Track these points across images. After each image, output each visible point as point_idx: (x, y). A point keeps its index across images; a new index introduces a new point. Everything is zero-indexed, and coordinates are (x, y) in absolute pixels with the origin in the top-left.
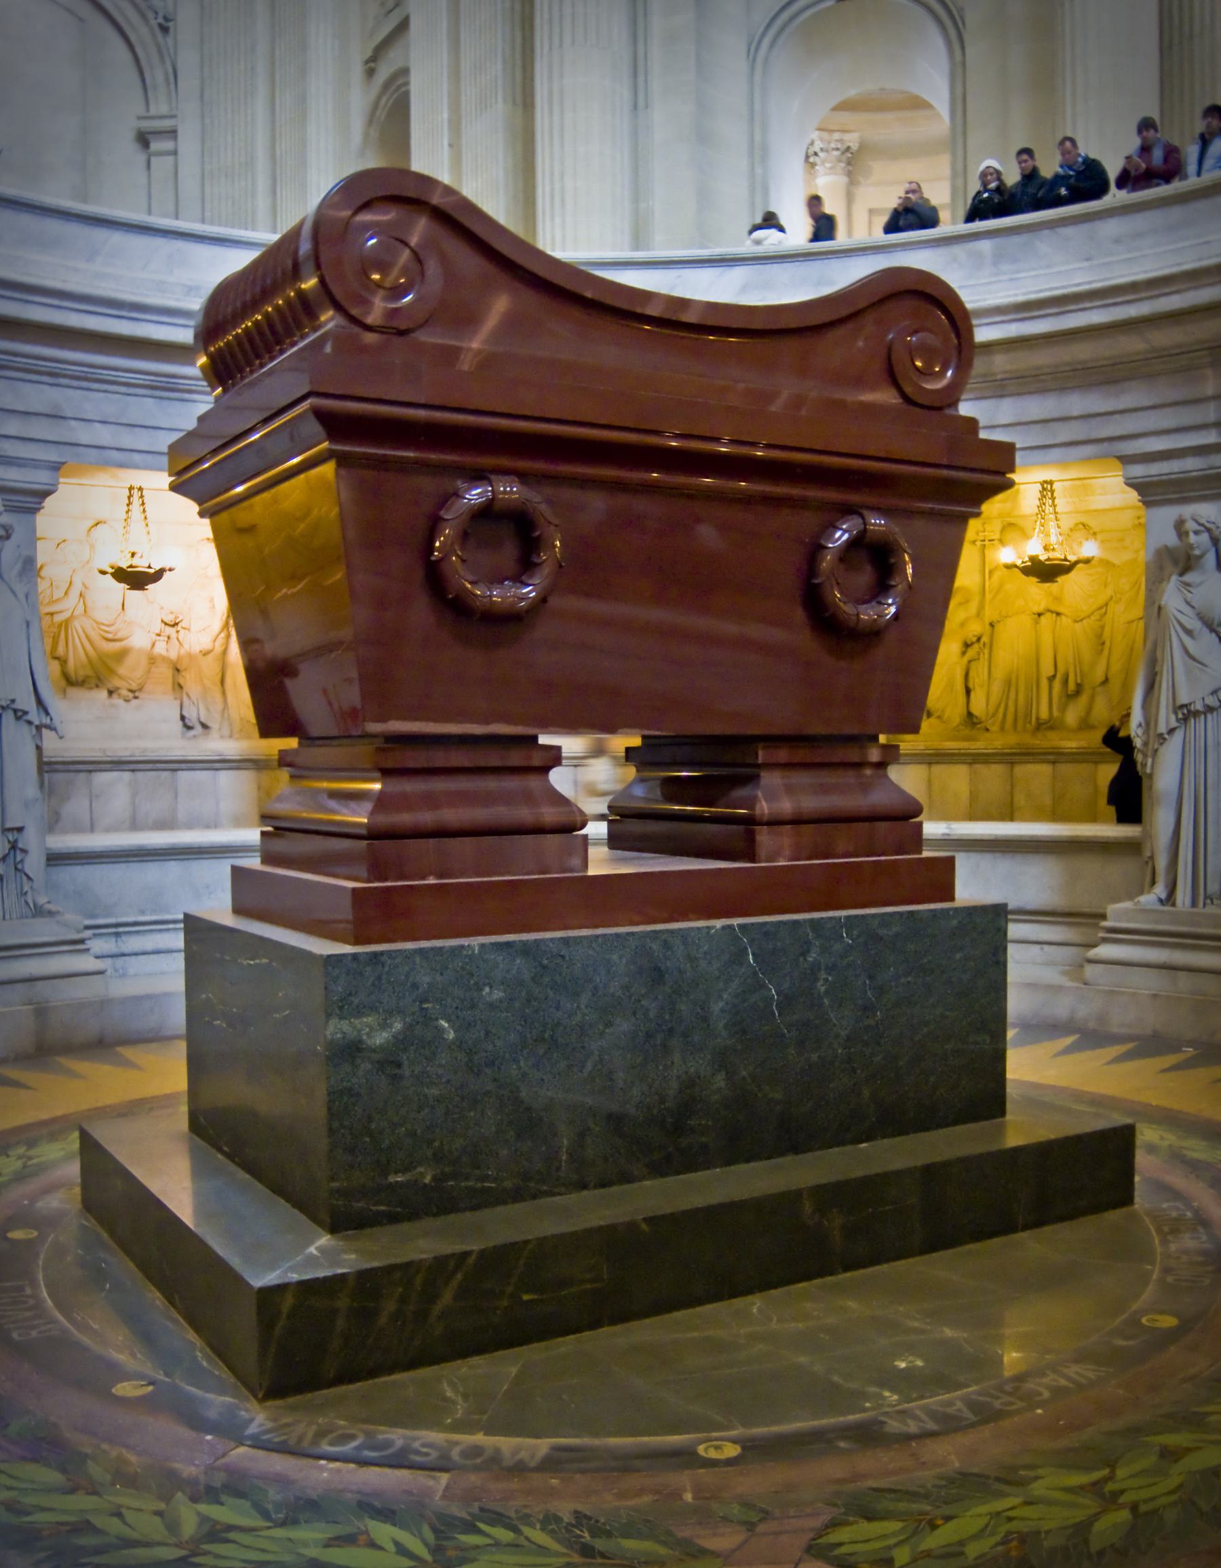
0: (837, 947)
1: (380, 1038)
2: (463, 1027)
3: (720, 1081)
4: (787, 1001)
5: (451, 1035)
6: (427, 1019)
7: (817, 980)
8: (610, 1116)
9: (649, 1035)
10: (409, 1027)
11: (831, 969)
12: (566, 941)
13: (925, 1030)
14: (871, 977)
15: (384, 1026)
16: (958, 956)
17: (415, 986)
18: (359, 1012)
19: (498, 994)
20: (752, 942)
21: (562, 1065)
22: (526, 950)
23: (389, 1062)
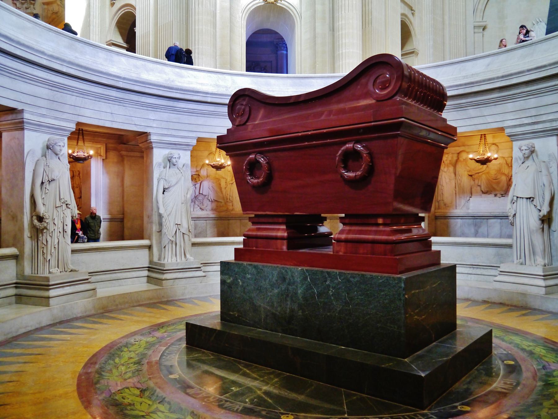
0: (336, 281)
1: (229, 281)
2: (243, 282)
3: (300, 313)
4: (320, 295)
5: (241, 283)
6: (237, 279)
7: (329, 290)
8: (273, 314)
9: (282, 295)
10: (234, 280)
11: (334, 288)
12: (263, 266)
13: (369, 316)
14: (348, 294)
15: (229, 279)
16: (382, 293)
17: (234, 271)
18: (226, 274)
19: (249, 276)
20: (309, 275)
21: (262, 297)
22: (255, 267)
23: (230, 286)
